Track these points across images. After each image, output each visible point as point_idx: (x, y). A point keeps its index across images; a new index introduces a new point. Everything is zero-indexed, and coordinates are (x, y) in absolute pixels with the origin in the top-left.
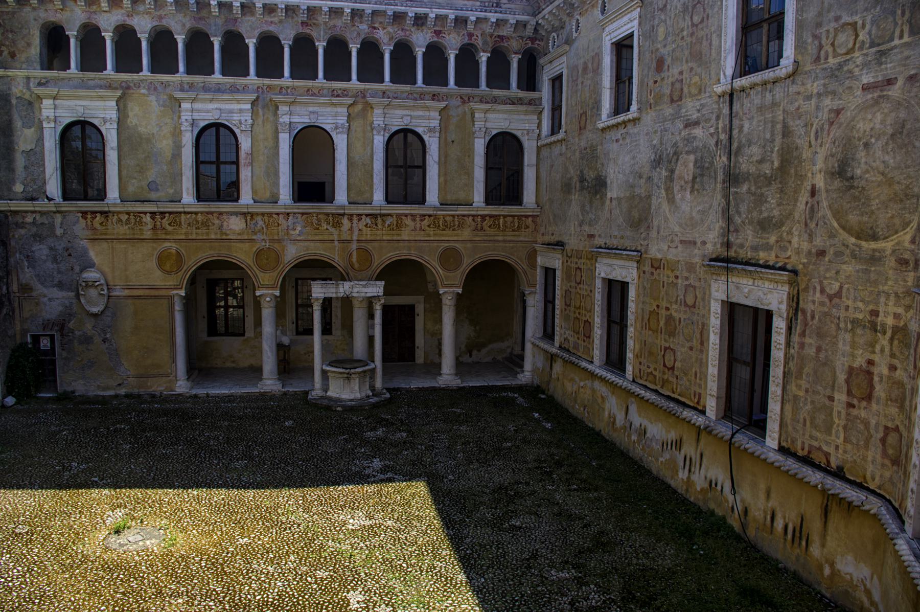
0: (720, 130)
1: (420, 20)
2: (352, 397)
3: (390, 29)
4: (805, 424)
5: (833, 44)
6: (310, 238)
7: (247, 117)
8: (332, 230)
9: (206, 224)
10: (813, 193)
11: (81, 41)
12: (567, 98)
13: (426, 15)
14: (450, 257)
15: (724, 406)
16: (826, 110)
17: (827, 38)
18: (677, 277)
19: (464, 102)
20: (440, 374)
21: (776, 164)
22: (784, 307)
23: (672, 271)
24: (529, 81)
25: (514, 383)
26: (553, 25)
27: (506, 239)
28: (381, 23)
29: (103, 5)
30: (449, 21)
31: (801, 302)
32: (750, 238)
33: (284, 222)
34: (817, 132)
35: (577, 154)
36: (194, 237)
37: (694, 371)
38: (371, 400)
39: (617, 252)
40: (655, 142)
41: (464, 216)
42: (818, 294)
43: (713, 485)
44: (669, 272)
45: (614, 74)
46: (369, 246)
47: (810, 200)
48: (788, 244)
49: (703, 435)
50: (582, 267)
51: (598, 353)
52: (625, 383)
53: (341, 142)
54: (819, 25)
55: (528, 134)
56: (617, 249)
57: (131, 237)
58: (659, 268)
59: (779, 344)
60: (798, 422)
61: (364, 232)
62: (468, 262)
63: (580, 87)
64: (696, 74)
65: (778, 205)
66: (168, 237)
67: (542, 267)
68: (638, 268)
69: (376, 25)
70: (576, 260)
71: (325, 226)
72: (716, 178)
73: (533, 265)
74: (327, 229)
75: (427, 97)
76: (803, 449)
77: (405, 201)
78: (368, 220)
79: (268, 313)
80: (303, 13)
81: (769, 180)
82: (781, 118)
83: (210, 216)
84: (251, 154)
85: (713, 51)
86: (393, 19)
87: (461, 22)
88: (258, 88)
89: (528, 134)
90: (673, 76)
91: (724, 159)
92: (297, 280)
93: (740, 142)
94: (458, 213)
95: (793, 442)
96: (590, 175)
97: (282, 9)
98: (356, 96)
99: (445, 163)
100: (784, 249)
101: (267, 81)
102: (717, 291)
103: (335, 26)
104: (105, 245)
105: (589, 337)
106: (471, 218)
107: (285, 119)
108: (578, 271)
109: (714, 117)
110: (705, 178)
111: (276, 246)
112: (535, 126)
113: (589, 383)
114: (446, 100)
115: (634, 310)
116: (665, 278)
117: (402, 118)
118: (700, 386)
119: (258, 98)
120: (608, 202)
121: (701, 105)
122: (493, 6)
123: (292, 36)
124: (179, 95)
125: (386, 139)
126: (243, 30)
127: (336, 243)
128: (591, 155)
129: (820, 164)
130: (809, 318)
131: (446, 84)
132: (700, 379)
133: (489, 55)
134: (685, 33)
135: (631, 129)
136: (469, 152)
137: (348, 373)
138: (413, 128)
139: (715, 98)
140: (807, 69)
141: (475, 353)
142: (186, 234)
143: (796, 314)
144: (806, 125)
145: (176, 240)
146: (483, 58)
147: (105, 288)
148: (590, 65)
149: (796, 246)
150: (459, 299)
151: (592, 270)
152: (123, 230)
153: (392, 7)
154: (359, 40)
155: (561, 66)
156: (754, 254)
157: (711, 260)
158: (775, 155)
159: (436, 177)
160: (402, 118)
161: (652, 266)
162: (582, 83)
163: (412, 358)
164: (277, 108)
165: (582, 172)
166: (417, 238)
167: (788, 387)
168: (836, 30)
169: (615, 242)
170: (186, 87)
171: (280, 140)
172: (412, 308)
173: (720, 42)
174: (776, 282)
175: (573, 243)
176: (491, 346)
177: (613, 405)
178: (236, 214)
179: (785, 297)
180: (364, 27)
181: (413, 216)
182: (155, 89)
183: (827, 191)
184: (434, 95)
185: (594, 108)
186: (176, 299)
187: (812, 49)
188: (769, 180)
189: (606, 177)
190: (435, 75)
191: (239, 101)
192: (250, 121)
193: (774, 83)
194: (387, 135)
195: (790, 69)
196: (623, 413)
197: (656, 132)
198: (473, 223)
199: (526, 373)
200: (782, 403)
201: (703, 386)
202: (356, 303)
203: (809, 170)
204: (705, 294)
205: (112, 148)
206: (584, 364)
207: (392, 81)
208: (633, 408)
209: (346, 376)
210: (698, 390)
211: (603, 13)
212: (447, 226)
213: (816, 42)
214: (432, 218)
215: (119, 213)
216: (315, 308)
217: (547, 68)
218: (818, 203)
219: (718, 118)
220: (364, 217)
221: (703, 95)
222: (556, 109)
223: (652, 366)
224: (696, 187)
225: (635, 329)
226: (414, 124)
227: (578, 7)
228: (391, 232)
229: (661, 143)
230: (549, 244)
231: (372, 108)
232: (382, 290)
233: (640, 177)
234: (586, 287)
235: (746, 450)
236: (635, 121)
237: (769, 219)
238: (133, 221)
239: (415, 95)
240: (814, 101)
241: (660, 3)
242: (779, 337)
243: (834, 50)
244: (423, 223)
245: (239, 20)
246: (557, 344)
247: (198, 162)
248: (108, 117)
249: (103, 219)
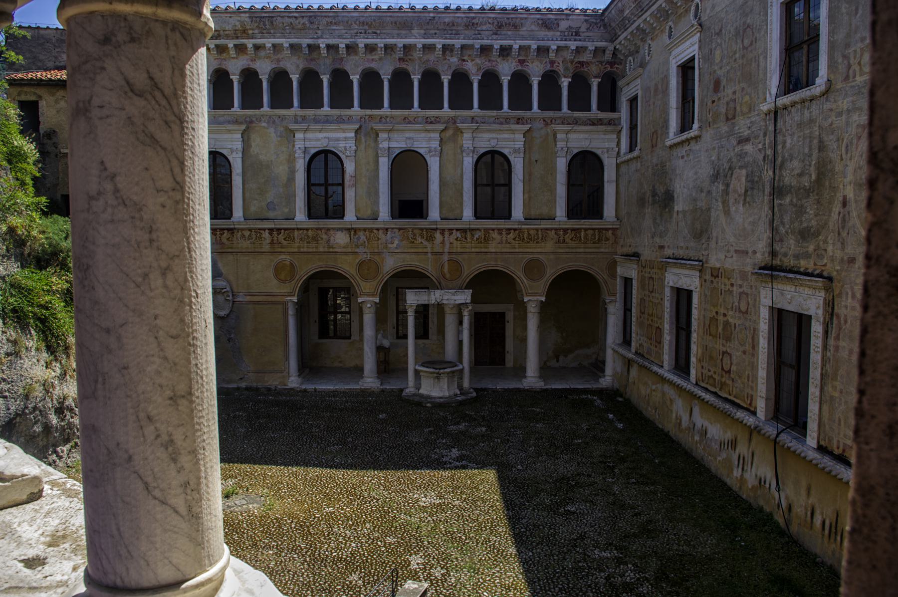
0: (767, 146)
1: (505, 51)
2: (441, 395)
3: (478, 61)
4: (840, 424)
5: (859, 64)
6: (406, 251)
7: (351, 144)
8: (426, 243)
9: (315, 239)
10: (845, 204)
11: (214, 84)
12: (642, 118)
13: (511, 47)
14: (533, 268)
15: (773, 408)
16: (855, 125)
17: (855, 58)
18: (732, 285)
19: (547, 124)
20: (525, 377)
21: (814, 177)
22: (820, 312)
23: (729, 279)
24: (609, 102)
25: (595, 386)
26: (629, 50)
27: (587, 250)
28: (469, 56)
29: (231, 52)
30: (532, 50)
31: (836, 307)
32: (792, 247)
33: (383, 236)
34: (847, 146)
35: (650, 170)
36: (305, 250)
37: (747, 373)
38: (458, 398)
39: (683, 262)
40: (713, 158)
41: (547, 229)
42: (850, 300)
43: (763, 483)
44: (726, 281)
45: (680, 95)
47: (842, 210)
48: (823, 252)
49: (755, 435)
50: (654, 276)
51: (667, 357)
52: (689, 386)
53: (434, 164)
54: (848, 46)
55: (607, 152)
56: (682, 259)
57: (253, 250)
58: (717, 276)
59: (817, 347)
60: (834, 421)
61: (455, 245)
62: (551, 273)
63: (652, 107)
64: (747, 94)
65: (816, 216)
66: (283, 250)
67: (621, 277)
68: (700, 277)
69: (465, 58)
70: (649, 270)
71: (419, 240)
72: (764, 191)
73: (613, 275)
74: (421, 243)
75: (512, 121)
76: (838, 448)
77: (492, 217)
78: (459, 234)
79: (369, 318)
80: (400, 51)
81: (808, 192)
82: (817, 133)
83: (319, 232)
84: (355, 177)
85: (761, 72)
86: (481, 52)
87: (542, 51)
88: (361, 118)
89: (607, 152)
90: (728, 95)
91: (771, 173)
92: (397, 288)
93: (783, 157)
94: (541, 226)
95: (830, 441)
96: (661, 190)
97: (381, 48)
98: (447, 122)
99: (530, 180)
100: (821, 257)
101: (368, 112)
102: (766, 298)
103: (428, 61)
104: (231, 257)
105: (660, 343)
106: (553, 232)
107: (384, 145)
108: (651, 280)
109: (762, 135)
110: (755, 191)
111: (377, 258)
112: (614, 145)
113: (659, 386)
114: (530, 123)
115: (696, 317)
116: (723, 286)
117: (489, 141)
118: (752, 388)
119: (360, 127)
120: (675, 215)
121: (751, 122)
123: (390, 71)
124: (293, 126)
125: (475, 160)
126: (348, 67)
127: (430, 255)
128: (662, 172)
129: (850, 177)
130: (842, 322)
131: (530, 108)
132: (752, 382)
133: (570, 80)
134: (737, 55)
135: (694, 146)
136: (553, 170)
137: (438, 373)
138: (499, 150)
139: (763, 116)
140: (838, 87)
141: (561, 358)
142: (299, 247)
143: (831, 319)
144: (838, 140)
145: (291, 253)
146: (565, 82)
147: (230, 294)
148: (660, 87)
149: (831, 254)
150: (543, 307)
151: (662, 280)
152: (245, 244)
153: (479, 41)
154: (450, 72)
155: (636, 88)
156: (796, 262)
157: (761, 268)
158: (812, 168)
159: (521, 194)
160: (489, 141)
161: (712, 275)
162: (654, 103)
163: (502, 361)
164: (377, 135)
165: (654, 187)
166: (503, 251)
167: (825, 388)
168: (862, 49)
169: (681, 253)
170: (299, 119)
171: (380, 164)
172: (502, 315)
173: (766, 63)
174: (814, 288)
175: (647, 254)
177: (679, 407)
178: (341, 230)
179: (821, 302)
180: (454, 60)
181: (500, 230)
182: (274, 122)
183: (856, 202)
184: (519, 119)
185: (663, 126)
186: (290, 304)
187: (842, 68)
188: (808, 192)
189: (673, 191)
190: (520, 99)
191: (344, 131)
192: (354, 148)
193: (811, 100)
194: (476, 157)
195: (823, 88)
196: (688, 414)
197: (714, 148)
198: (556, 236)
199: (607, 378)
200: (820, 403)
201: (755, 388)
202: (447, 310)
203: (841, 182)
204: (755, 300)
205: (238, 174)
206: (655, 368)
207: (480, 107)
208: (696, 410)
209: (435, 375)
210: (751, 392)
211: (670, 38)
212: (531, 239)
213: (845, 62)
214: (517, 232)
215: (243, 229)
216: (409, 314)
217: (625, 90)
218: (849, 213)
219: (765, 134)
220: (454, 231)
221: (753, 114)
222: (633, 128)
223: (712, 370)
224: (748, 200)
225: (698, 334)
226: (500, 146)
227: (649, 33)
229: (719, 159)
230: (626, 255)
231: (462, 132)
232: (469, 298)
233: (702, 191)
234: (657, 295)
235: (789, 448)
236: (697, 138)
237: (808, 229)
238: (254, 236)
239: (501, 120)
240: (844, 117)
241: (716, 28)
242: (816, 341)
243: (861, 69)
245: (345, 59)
246: (633, 350)
247: (310, 185)
248: (235, 147)
249: (229, 235)
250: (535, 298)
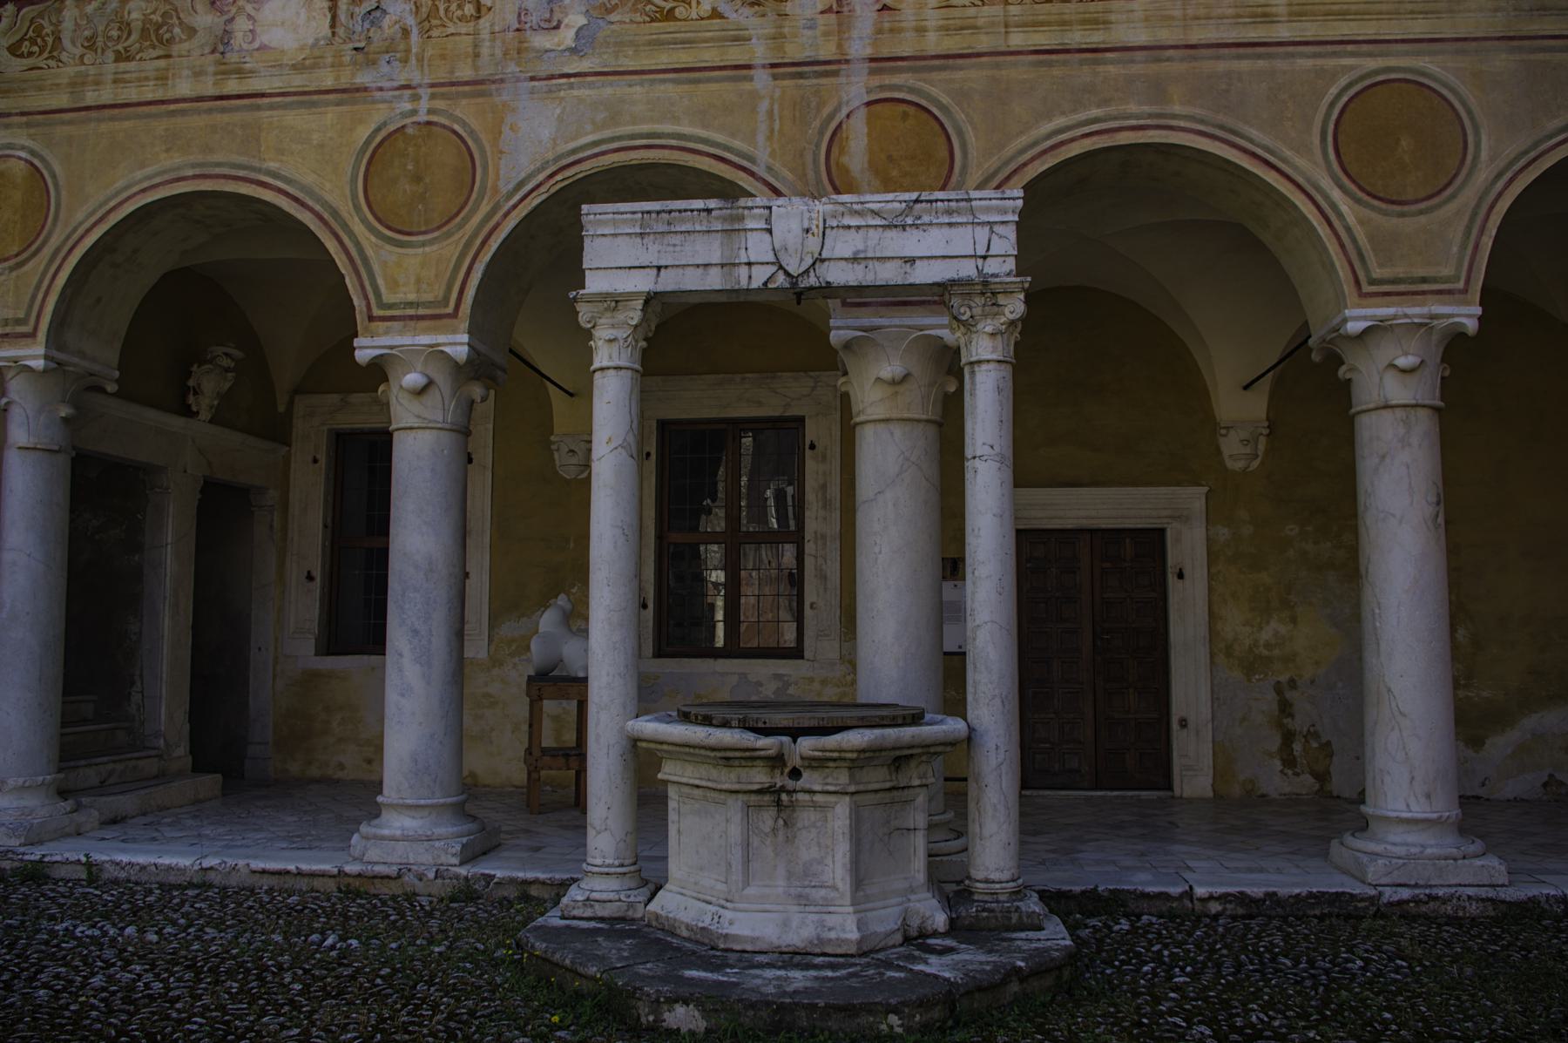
2: (800, 932)
20: (1362, 825)
36: (106, 95)
38: (935, 966)
46: (936, 88)
111: (466, 112)
127: (761, 79)
137: (776, 761)
142: (77, 84)
163: (1159, 773)
166: (1196, 36)
172: (1151, 542)
176: (1530, 722)
186: (17, 388)
209: (759, 777)
216: (603, 356)
232: (1006, 242)
250: (1416, 311)
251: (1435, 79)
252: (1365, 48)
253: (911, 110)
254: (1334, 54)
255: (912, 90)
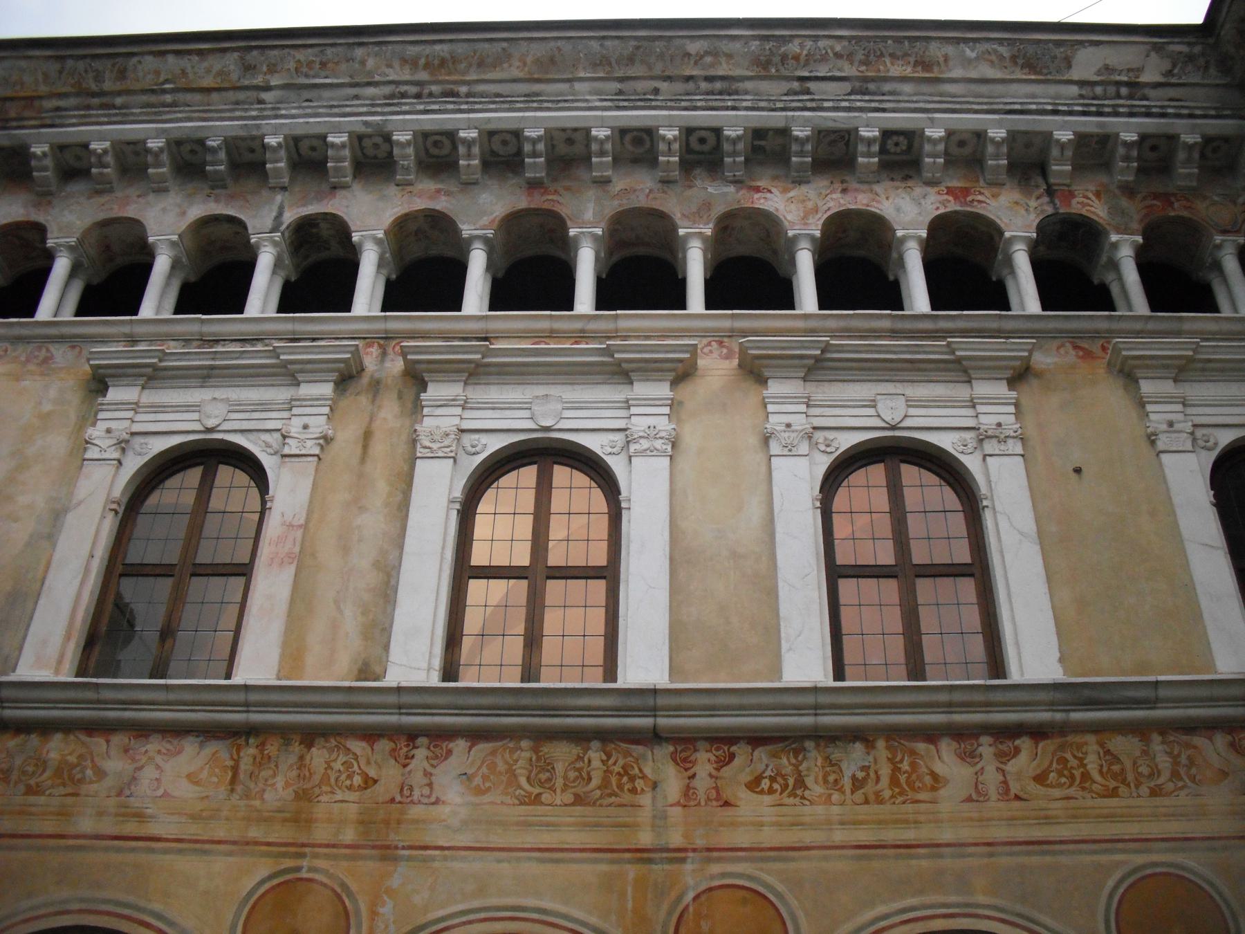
6: (497, 840)
46: (769, 877)
84: (305, 527)
122: (1118, 96)
212: (1121, 777)
228: (874, 808)
244: (1012, 767)
251: (1195, 873)
252: (1132, 845)
253: (748, 895)
254: (1106, 851)
255: (750, 878)
